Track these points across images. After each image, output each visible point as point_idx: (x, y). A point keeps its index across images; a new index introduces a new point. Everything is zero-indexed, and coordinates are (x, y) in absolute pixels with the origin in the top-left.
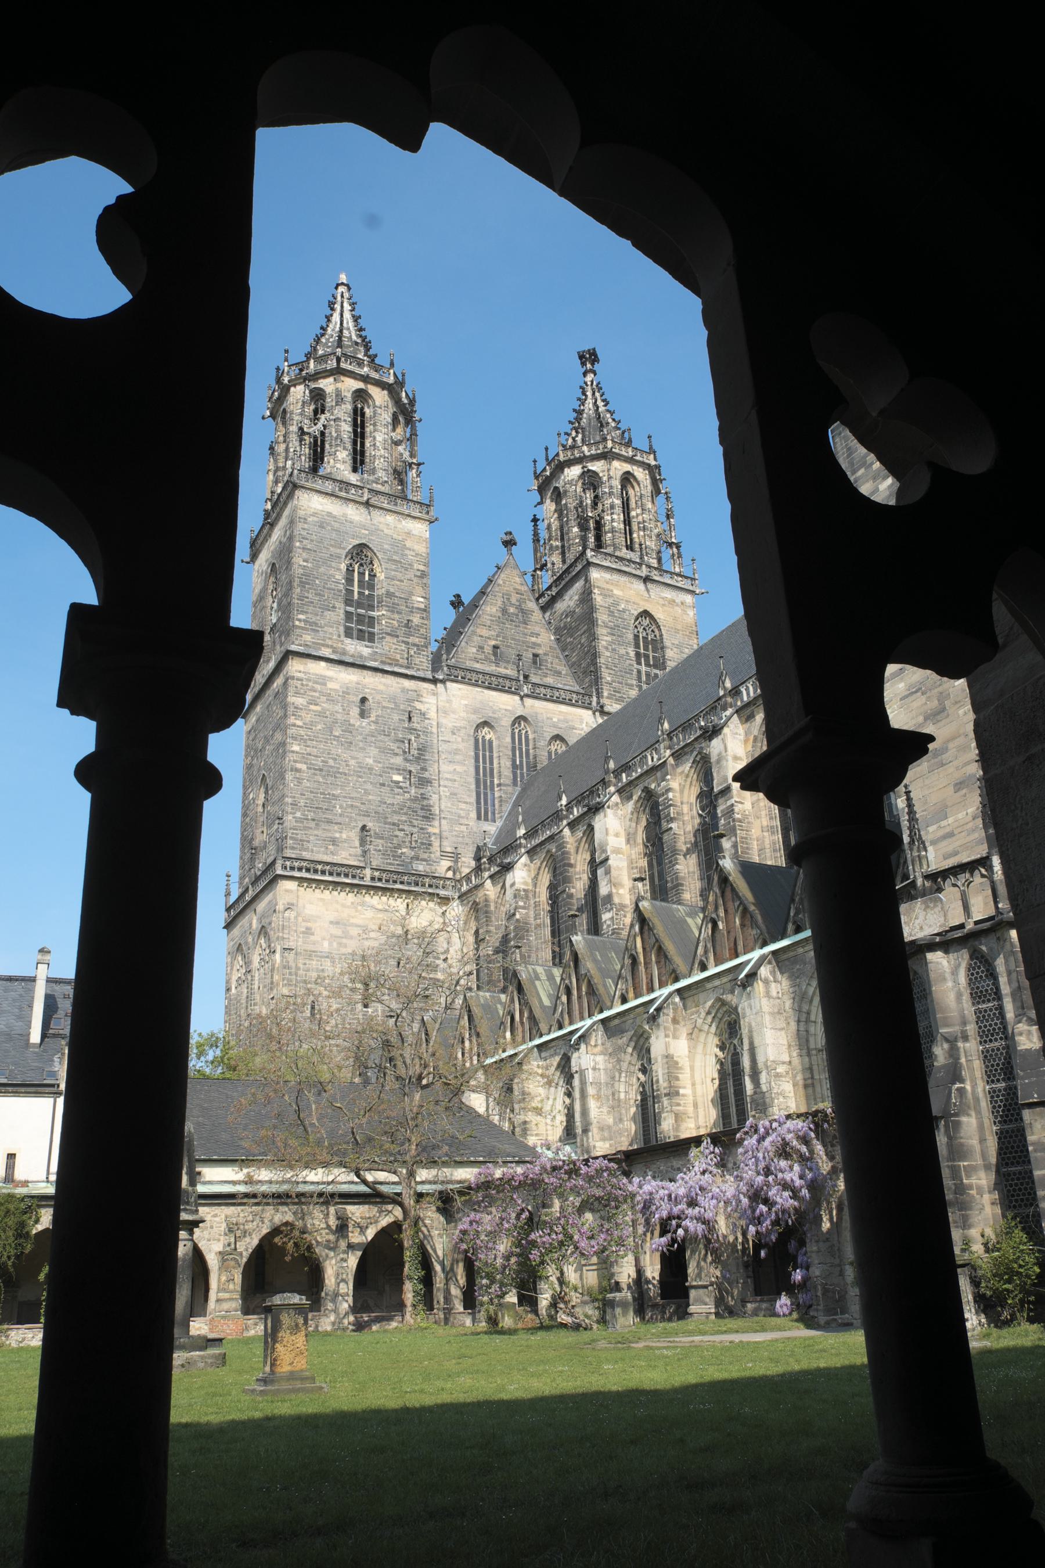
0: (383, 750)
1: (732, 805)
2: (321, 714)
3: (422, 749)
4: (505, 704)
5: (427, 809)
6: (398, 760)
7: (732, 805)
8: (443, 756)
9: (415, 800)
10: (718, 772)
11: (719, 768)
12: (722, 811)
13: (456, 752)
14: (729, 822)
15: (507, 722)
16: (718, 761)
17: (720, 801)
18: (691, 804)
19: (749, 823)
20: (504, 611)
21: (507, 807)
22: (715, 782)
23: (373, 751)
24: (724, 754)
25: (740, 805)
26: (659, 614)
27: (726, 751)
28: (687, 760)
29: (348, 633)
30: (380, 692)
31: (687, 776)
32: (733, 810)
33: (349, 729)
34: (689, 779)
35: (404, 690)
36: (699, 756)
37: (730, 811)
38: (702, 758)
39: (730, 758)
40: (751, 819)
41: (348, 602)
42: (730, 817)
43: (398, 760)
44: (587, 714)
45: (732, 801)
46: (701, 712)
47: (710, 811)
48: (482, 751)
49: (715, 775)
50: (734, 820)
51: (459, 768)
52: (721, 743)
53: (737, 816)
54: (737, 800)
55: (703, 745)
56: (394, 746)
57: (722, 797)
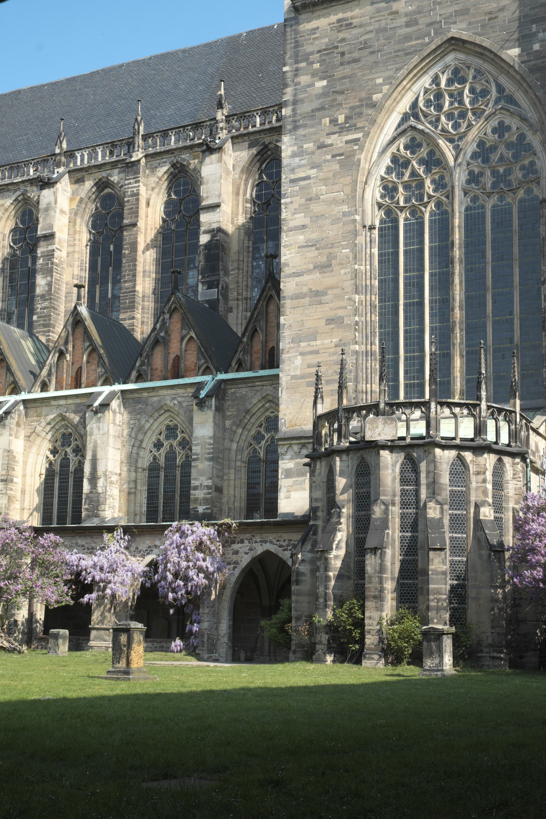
1: (53, 250)
7: (53, 250)
10: (45, 219)
11: (47, 215)
12: (42, 252)
14: (48, 264)
16: (47, 210)
17: (42, 243)
18: (4, 235)
19: (62, 268)
22: (40, 226)
24: (53, 205)
25: (58, 252)
27: (56, 203)
28: (9, 197)
31: (6, 210)
32: (53, 255)
34: (7, 214)
36: (21, 197)
37: (50, 255)
38: (24, 199)
39: (58, 210)
40: (65, 266)
42: (49, 260)
45: (54, 247)
46: (33, 160)
47: (22, 246)
49: (41, 220)
50: (52, 263)
52: (52, 195)
53: (55, 261)
54: (58, 247)
55: (28, 189)
57: (44, 241)
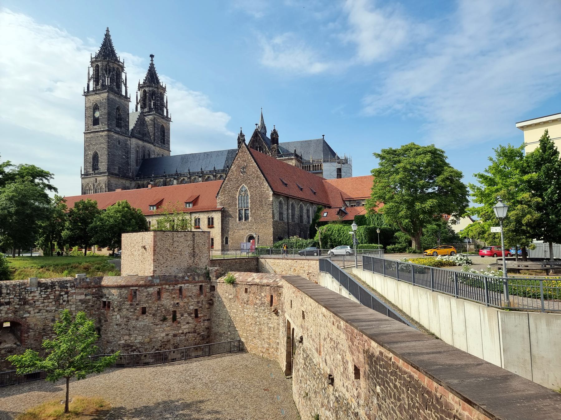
0: (122, 151)
2: (112, 143)
3: (128, 151)
4: (140, 143)
5: (128, 163)
6: (124, 153)
8: (131, 153)
9: (126, 161)
13: (133, 152)
15: (141, 147)
20: (141, 123)
21: (141, 164)
23: (121, 151)
26: (164, 126)
29: (117, 127)
30: (122, 139)
33: (117, 147)
35: (125, 139)
41: (117, 119)
43: (124, 153)
44: (152, 146)
48: (137, 152)
51: (134, 156)
56: (123, 150)
